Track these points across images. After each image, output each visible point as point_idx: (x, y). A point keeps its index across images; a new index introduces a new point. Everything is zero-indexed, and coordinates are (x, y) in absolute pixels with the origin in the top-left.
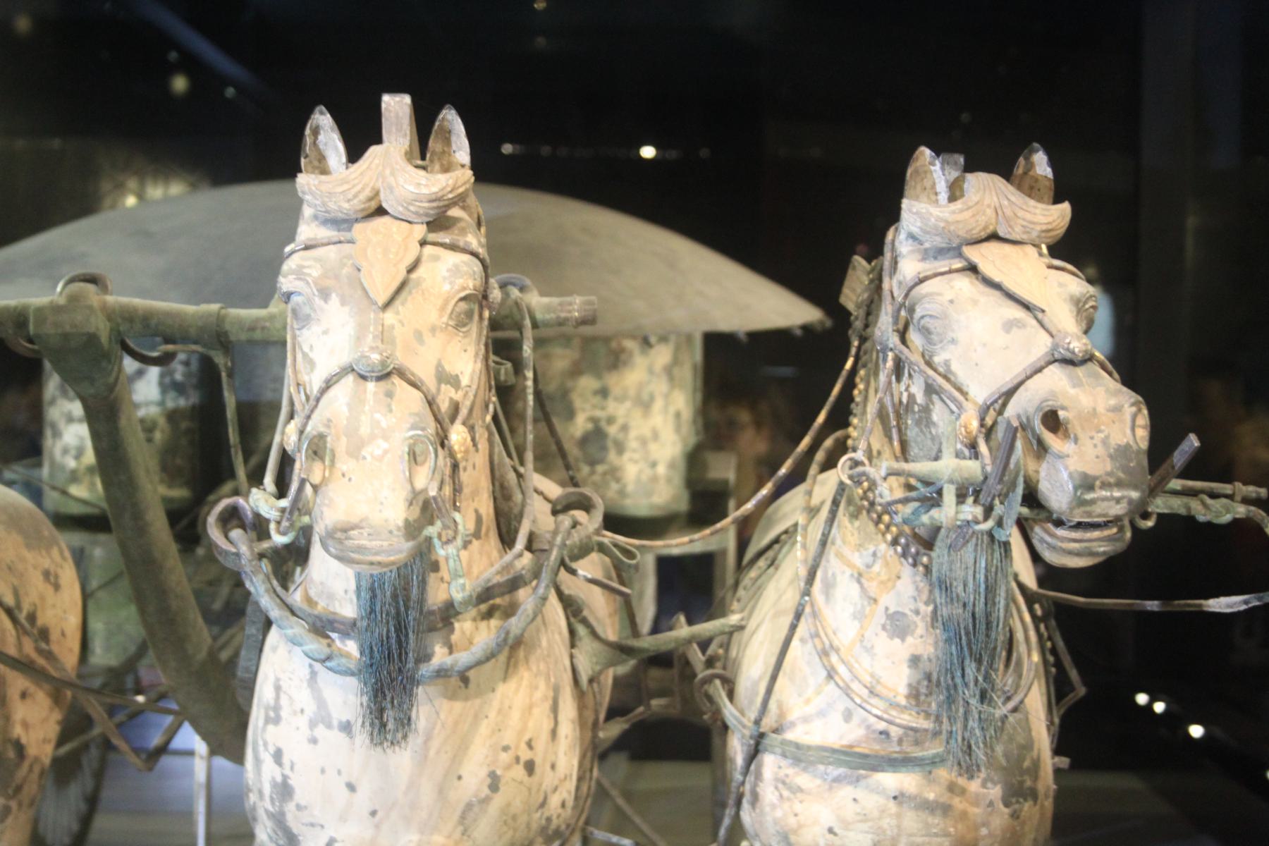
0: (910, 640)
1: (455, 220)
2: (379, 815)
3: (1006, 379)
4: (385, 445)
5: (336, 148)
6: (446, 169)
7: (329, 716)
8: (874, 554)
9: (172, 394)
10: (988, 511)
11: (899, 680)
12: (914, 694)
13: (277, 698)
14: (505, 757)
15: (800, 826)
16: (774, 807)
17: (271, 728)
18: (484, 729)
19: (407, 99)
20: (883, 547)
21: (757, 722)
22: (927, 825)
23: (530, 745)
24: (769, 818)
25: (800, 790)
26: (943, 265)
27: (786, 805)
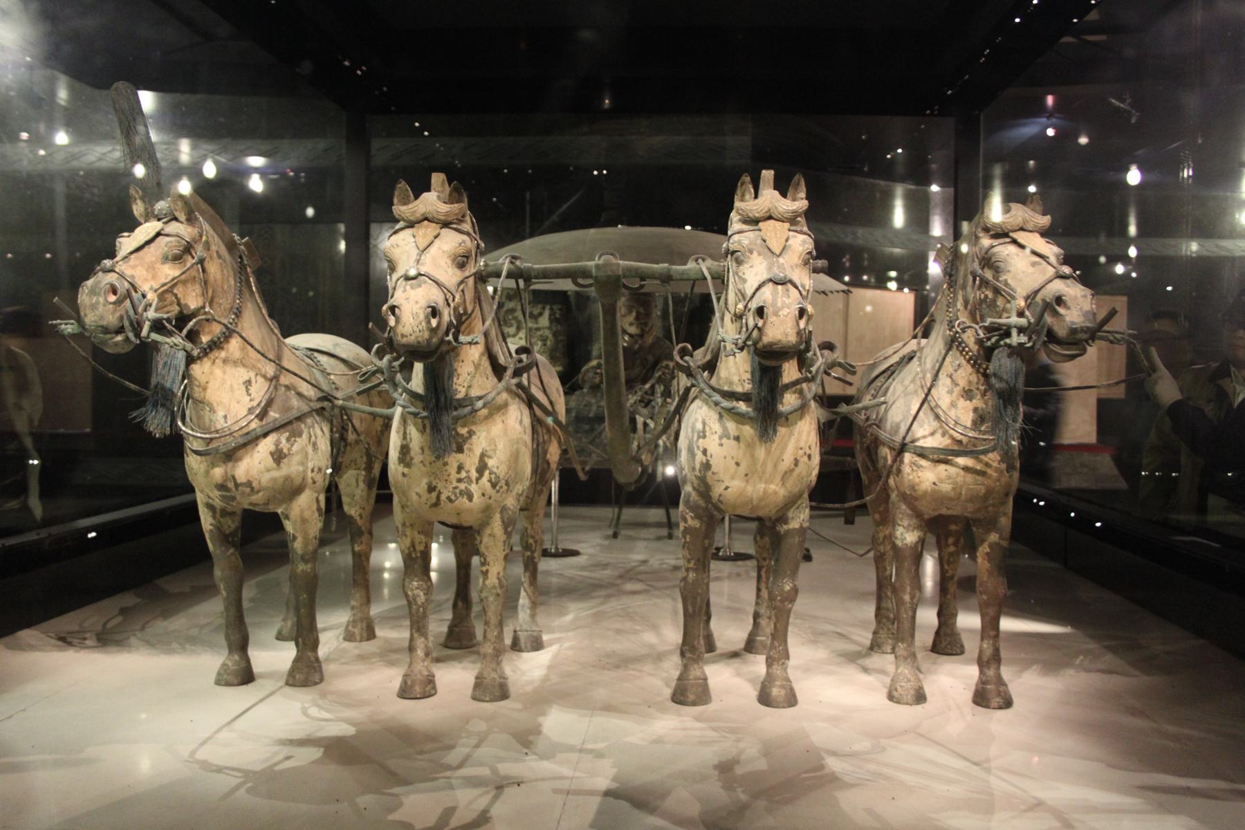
0: (974, 401)
1: (799, 221)
2: (749, 476)
3: (1036, 286)
4: (788, 311)
5: (750, 191)
6: (794, 200)
7: (729, 434)
8: (959, 365)
9: (555, 324)
10: (1030, 339)
11: (967, 418)
12: (974, 423)
13: (704, 427)
14: (801, 452)
15: (920, 482)
16: (909, 474)
17: (701, 440)
18: (793, 440)
19: (764, 171)
20: (964, 362)
21: (904, 438)
22: (976, 480)
23: (810, 448)
24: (906, 480)
25: (922, 466)
26: (1002, 241)
27: (915, 474)
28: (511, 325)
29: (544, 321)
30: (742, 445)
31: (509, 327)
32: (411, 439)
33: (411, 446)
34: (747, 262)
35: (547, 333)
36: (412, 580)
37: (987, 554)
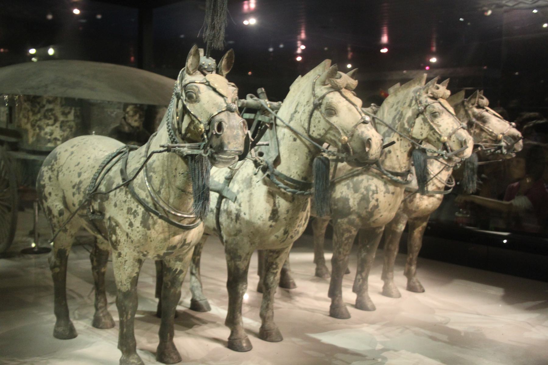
16: (418, 202)
28: (50, 119)
29: (71, 117)
30: (394, 196)
33: (279, 209)
34: (440, 117)
35: (73, 124)
36: (243, 285)
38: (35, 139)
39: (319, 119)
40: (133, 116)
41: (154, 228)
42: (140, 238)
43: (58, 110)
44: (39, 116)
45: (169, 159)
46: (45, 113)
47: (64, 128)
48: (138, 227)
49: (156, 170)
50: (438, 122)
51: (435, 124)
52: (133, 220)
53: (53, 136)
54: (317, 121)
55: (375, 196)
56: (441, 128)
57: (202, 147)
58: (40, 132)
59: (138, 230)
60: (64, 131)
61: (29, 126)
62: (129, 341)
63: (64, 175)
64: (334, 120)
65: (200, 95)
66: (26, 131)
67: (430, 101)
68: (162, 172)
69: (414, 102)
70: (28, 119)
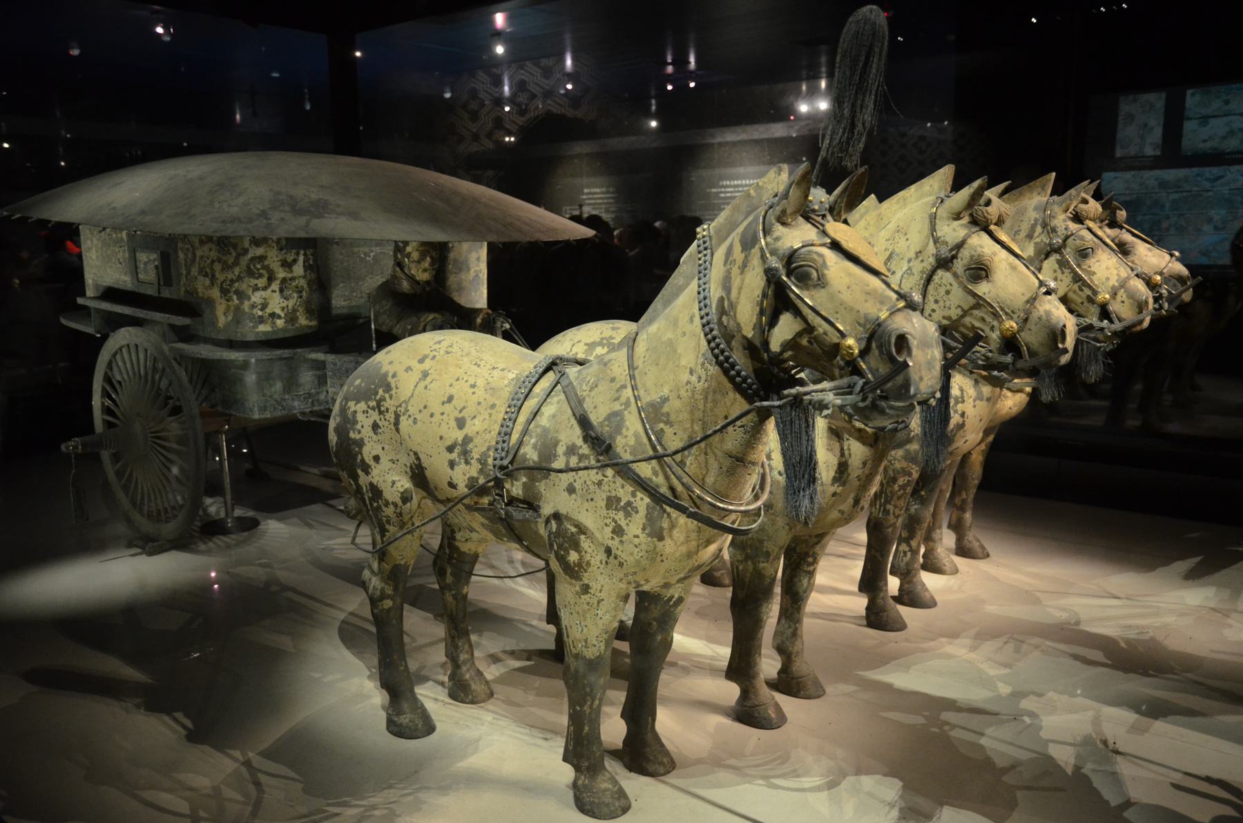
13: (962, 394)
28: (261, 276)
29: (299, 269)
31: (257, 278)
32: (850, 455)
34: (1093, 257)
37: (982, 451)
38: (230, 318)
39: (949, 287)
40: (419, 262)
41: (670, 536)
42: (642, 557)
43: (274, 258)
44: (237, 271)
45: (710, 398)
46: (248, 267)
47: (287, 293)
48: (637, 537)
49: (673, 417)
50: (1090, 267)
51: (1083, 270)
52: (623, 523)
53: (268, 310)
54: (942, 291)
55: (960, 407)
56: (1094, 278)
57: (858, 388)
58: (242, 303)
59: (636, 541)
60: (287, 299)
61: (215, 293)
62: (594, 749)
63: (415, 422)
64: (983, 289)
65: (826, 272)
66: (210, 302)
67: (1073, 226)
68: (689, 422)
69: (1039, 229)
70: (213, 278)
